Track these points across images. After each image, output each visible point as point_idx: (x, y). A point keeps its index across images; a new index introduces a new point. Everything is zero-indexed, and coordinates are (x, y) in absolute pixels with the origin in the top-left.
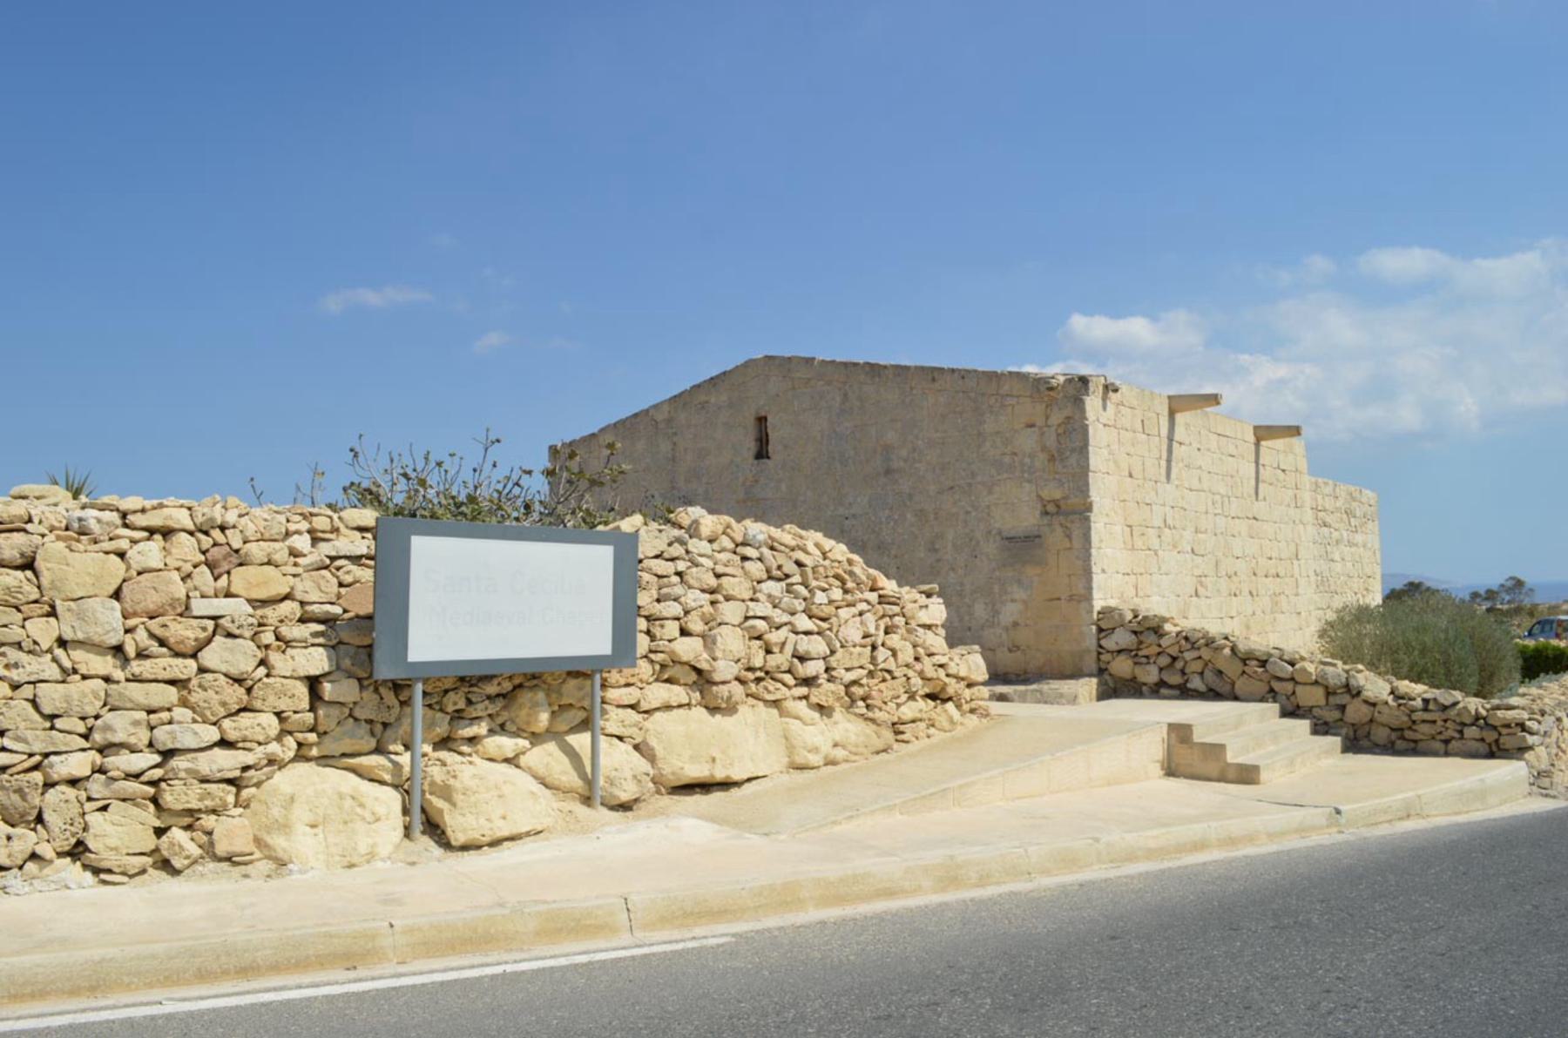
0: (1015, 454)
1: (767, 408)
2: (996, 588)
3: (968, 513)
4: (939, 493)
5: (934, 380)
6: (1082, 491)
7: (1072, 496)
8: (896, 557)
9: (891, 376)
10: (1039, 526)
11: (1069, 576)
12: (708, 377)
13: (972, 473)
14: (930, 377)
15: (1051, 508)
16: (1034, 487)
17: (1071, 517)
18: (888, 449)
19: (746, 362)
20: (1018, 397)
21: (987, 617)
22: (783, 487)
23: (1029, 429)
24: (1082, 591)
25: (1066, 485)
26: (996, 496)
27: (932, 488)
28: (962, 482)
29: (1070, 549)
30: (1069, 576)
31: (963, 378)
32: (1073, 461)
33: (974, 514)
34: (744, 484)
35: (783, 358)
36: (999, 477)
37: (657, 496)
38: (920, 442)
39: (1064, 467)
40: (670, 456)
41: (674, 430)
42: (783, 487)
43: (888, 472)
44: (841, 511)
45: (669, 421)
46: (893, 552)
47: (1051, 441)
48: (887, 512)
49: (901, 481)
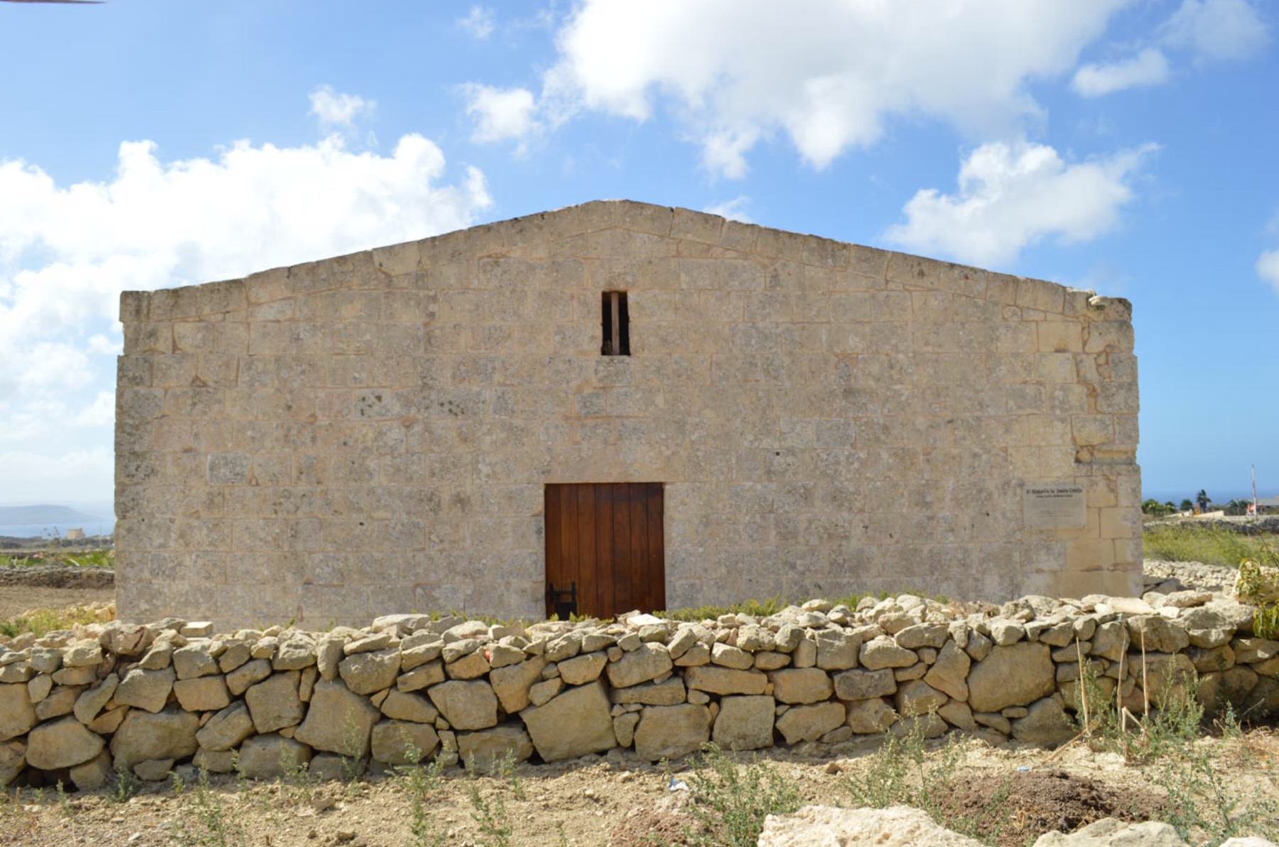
0: (1040, 383)
1: (629, 279)
2: (1016, 556)
3: (975, 455)
4: (931, 426)
5: (921, 274)
6: (1130, 437)
7: (1117, 442)
8: (862, 511)
9: (853, 261)
10: (1075, 477)
11: (1113, 540)
12: (512, 217)
13: (980, 404)
14: (916, 270)
15: (1085, 456)
16: (1069, 427)
17: (1117, 468)
18: (847, 360)
19: (588, 204)
20: (1045, 312)
21: (1003, 594)
22: (660, 400)
23: (1060, 355)
24: (1131, 559)
25: (1110, 428)
26: (1014, 437)
27: (921, 422)
28: (967, 414)
29: (1116, 506)
30: (1113, 540)
31: (967, 277)
32: (1119, 398)
33: (984, 457)
34: (579, 390)
35: (659, 209)
36: (1021, 412)
37: (387, 395)
38: (901, 356)
39: (1109, 406)
40: (420, 333)
41: (432, 293)
42: (660, 400)
43: (849, 392)
44: (766, 443)
45: (420, 278)
46: (858, 505)
47: (1091, 374)
48: (848, 447)
49: (870, 406)
